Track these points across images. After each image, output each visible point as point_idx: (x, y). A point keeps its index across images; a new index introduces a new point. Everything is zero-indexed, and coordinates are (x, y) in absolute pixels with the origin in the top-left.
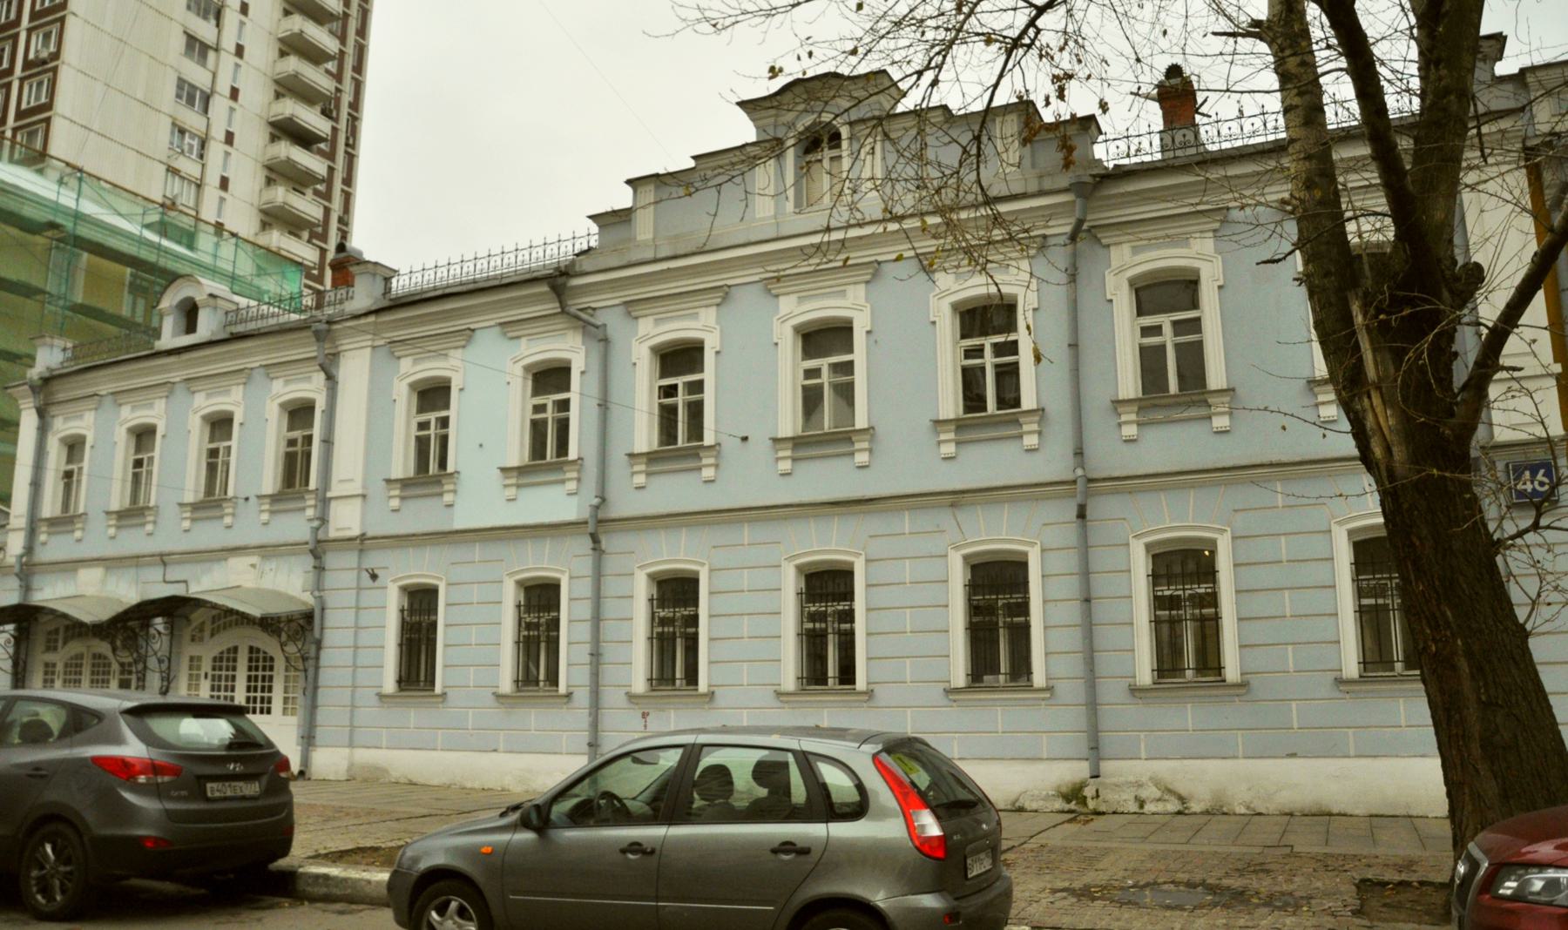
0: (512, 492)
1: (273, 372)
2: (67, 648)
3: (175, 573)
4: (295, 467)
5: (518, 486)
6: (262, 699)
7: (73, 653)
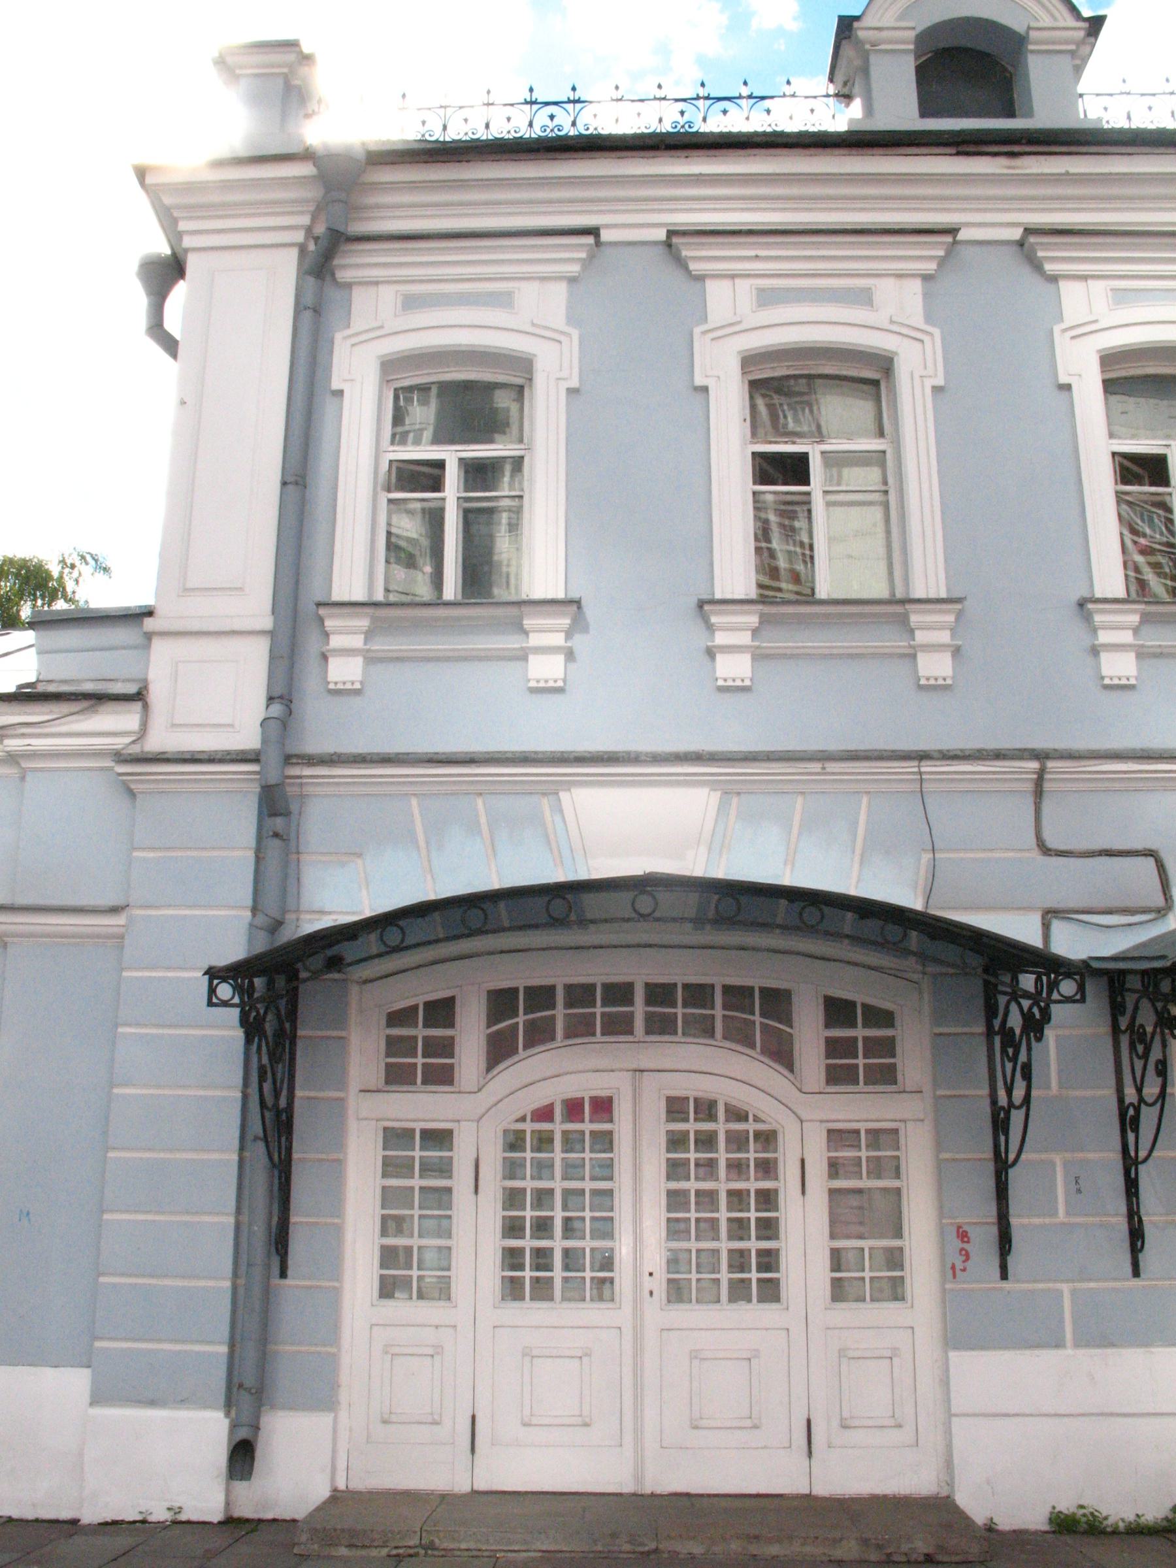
2: (512, 1073)
7: (555, 1092)
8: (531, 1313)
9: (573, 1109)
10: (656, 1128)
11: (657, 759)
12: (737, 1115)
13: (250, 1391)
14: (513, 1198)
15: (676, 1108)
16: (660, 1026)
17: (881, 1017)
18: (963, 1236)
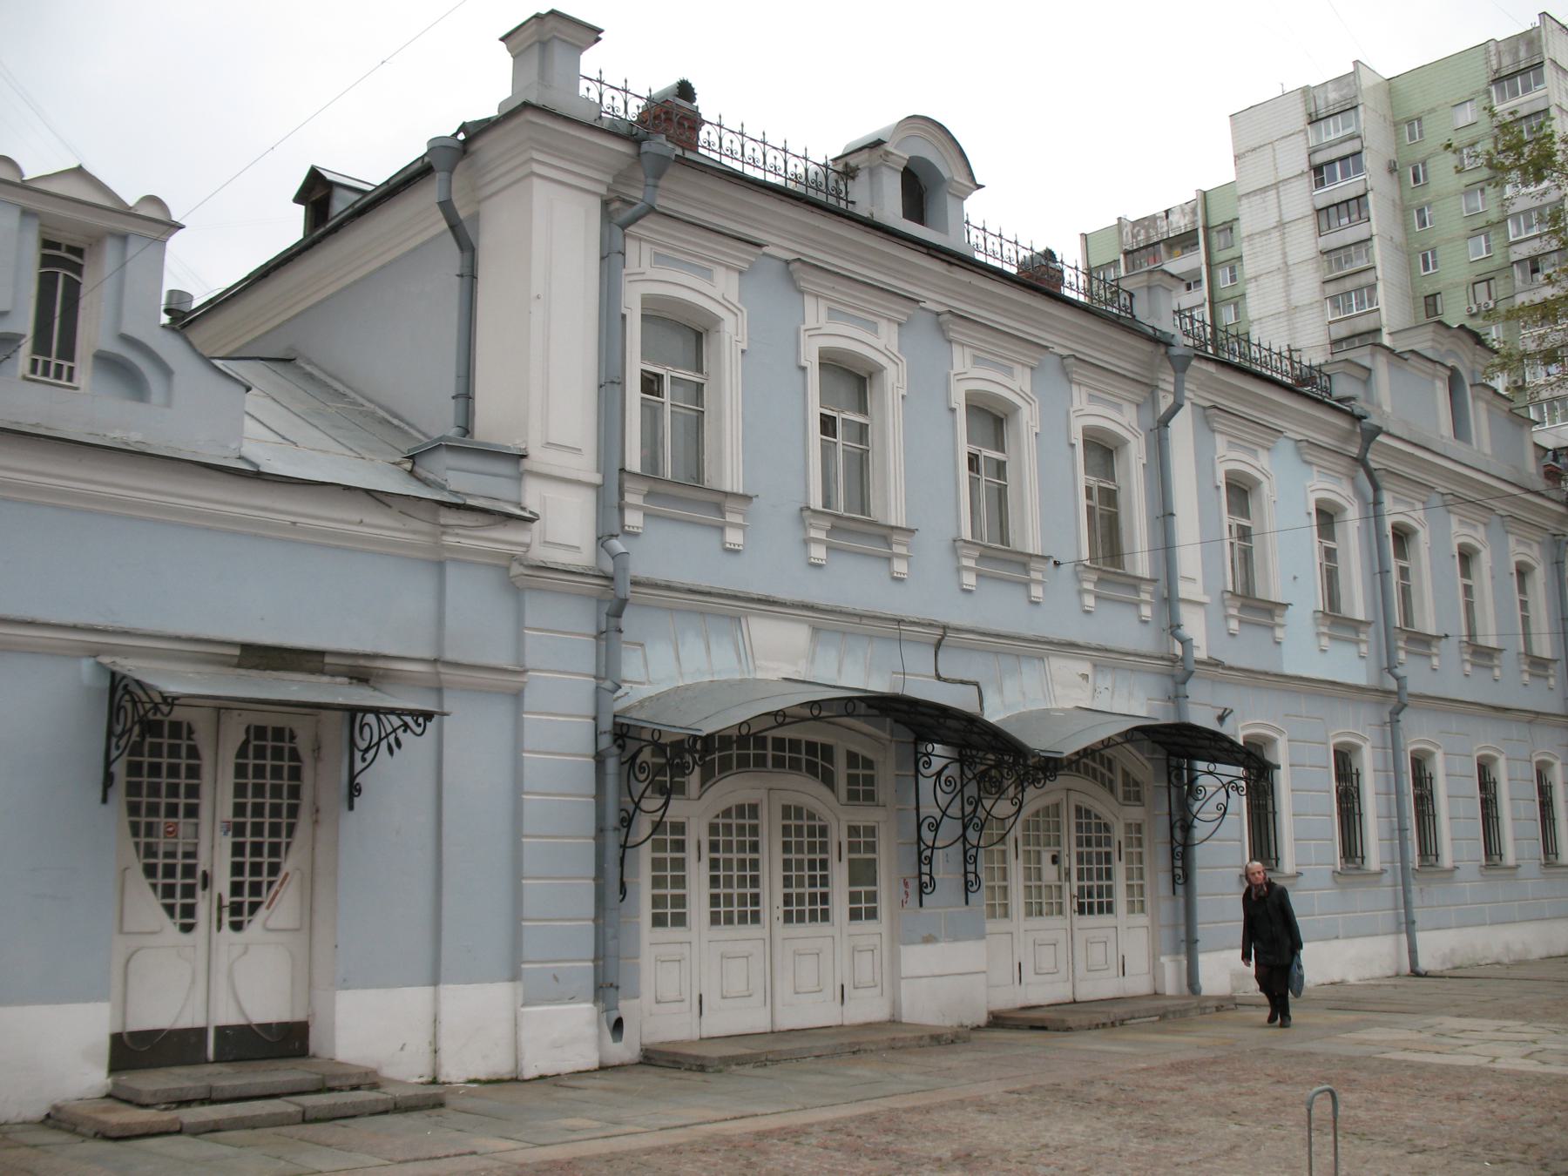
0: (1325, 641)
3: (952, 665)
5: (1332, 638)
7: (733, 800)
8: (724, 931)
9: (741, 810)
10: (779, 823)
11: (794, 605)
14: (714, 864)
16: (779, 763)
17: (869, 764)
18: (906, 884)
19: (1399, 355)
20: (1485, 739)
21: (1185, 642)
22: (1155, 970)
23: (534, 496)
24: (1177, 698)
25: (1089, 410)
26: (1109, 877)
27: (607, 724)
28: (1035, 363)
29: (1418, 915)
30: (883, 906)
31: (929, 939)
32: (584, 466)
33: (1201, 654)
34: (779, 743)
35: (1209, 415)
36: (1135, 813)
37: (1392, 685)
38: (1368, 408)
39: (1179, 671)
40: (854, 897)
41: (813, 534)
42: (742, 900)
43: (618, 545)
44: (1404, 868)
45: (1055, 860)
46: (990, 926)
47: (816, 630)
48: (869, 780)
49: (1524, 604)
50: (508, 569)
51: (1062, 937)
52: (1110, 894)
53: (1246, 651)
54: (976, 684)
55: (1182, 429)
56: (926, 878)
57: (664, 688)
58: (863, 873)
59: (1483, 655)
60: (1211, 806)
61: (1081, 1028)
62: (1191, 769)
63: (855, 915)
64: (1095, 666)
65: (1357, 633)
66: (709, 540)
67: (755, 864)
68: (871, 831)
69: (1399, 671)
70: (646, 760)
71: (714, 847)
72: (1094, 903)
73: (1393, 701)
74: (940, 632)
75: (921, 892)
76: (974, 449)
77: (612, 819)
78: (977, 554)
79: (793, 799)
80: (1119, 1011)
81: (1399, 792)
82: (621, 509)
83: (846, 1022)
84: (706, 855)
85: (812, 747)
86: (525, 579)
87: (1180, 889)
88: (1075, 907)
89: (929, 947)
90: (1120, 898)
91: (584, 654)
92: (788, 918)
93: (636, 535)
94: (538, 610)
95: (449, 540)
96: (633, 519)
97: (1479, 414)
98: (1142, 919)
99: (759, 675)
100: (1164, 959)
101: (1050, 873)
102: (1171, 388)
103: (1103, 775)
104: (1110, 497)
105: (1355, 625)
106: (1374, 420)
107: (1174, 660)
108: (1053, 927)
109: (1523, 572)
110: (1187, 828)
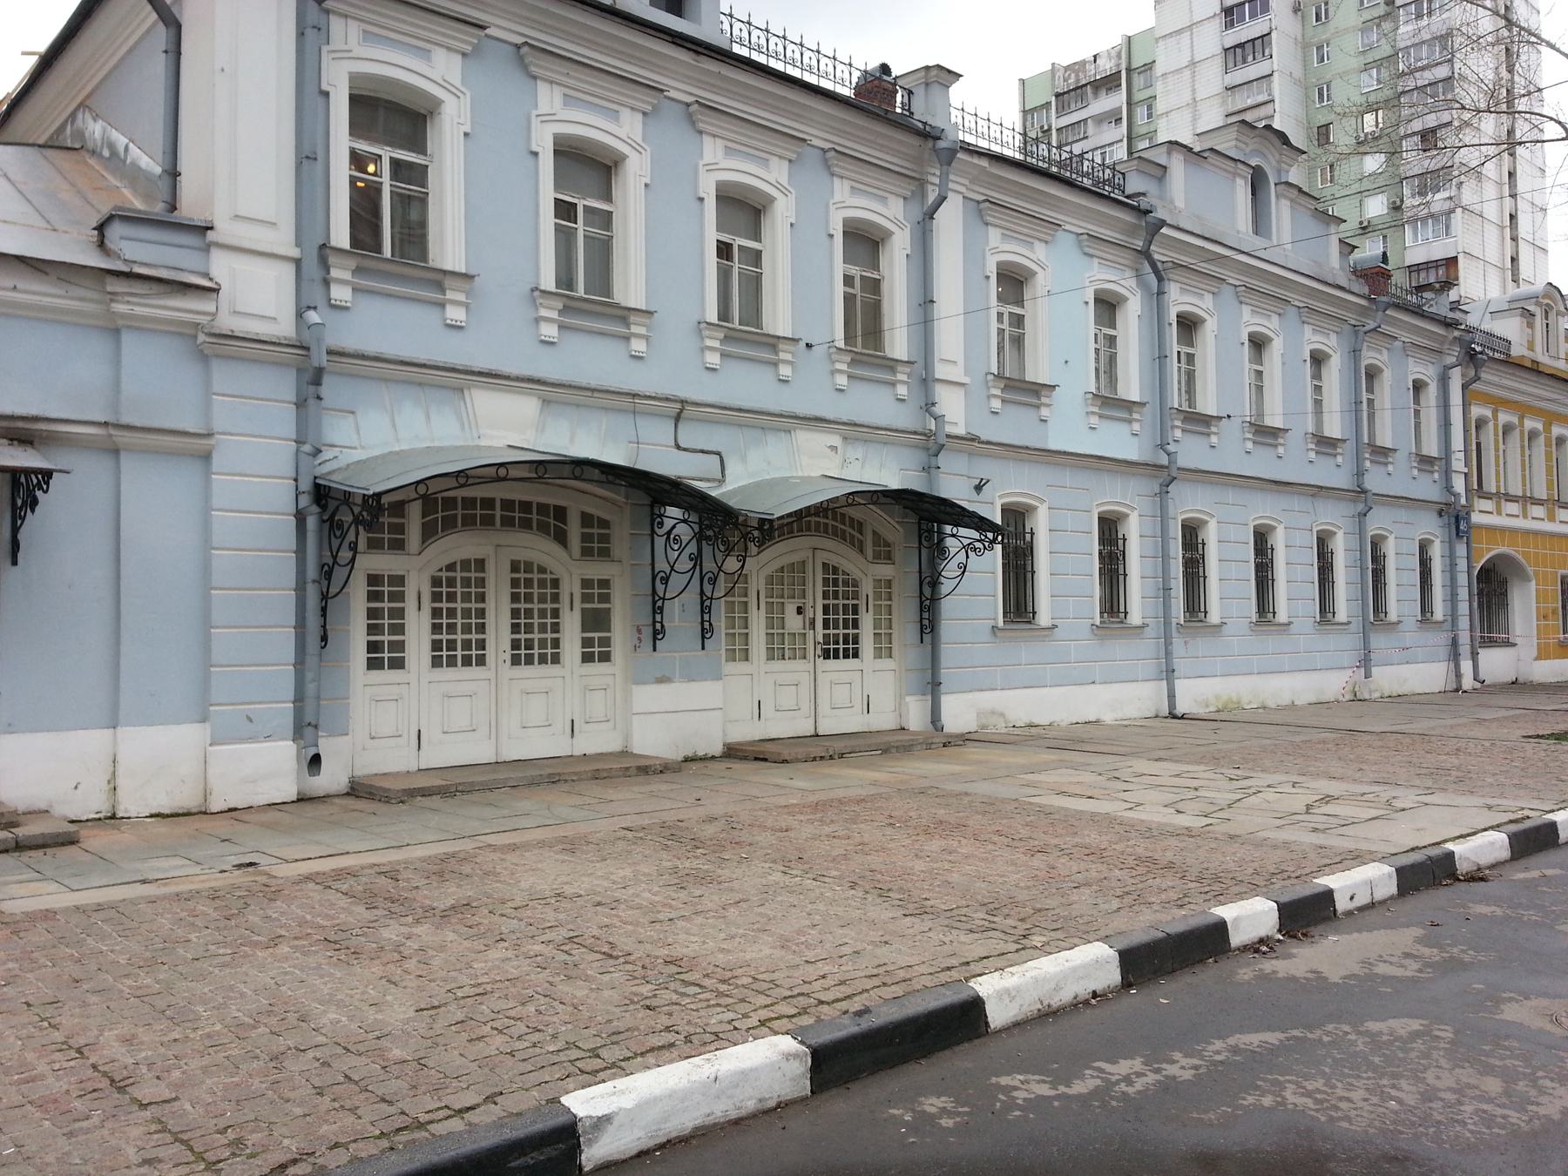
0: (1094, 420)
1: (840, 166)
3: (691, 435)
4: (865, 317)
5: (1101, 416)
6: (846, 637)
8: (447, 673)
9: (466, 564)
10: (507, 576)
11: (518, 379)
12: (542, 570)
13: (304, 727)
14: (436, 613)
15: (515, 567)
16: (508, 522)
17: (604, 524)
18: (639, 631)
19: (1197, 154)
20: (1262, 509)
21: (938, 418)
22: (900, 710)
23: (221, 267)
24: (929, 469)
25: (847, 201)
26: (856, 626)
27: (306, 485)
28: (793, 157)
29: (1178, 664)
30: (618, 648)
31: (662, 680)
32: (283, 240)
33: (960, 430)
34: (469, 503)
35: (982, 210)
36: (885, 571)
37: (1164, 460)
38: (1154, 201)
39: (932, 444)
40: (587, 642)
41: (543, 313)
42: (467, 645)
43: (313, 317)
44: (1167, 623)
45: (800, 611)
46: (730, 668)
47: (546, 402)
48: (605, 539)
49: (1318, 389)
50: (196, 337)
51: (806, 679)
52: (856, 641)
53: (1014, 426)
54: (718, 454)
55: (951, 220)
56: (658, 626)
57: (377, 452)
58: (596, 621)
59: (1266, 434)
60: (953, 565)
61: (798, 760)
62: (940, 532)
63: (587, 658)
64: (845, 438)
65: (1130, 412)
66: (429, 316)
67: (481, 613)
68: (605, 583)
69: (1171, 448)
70: (341, 520)
71: (436, 597)
72: (842, 647)
73: (1163, 475)
74: (679, 406)
75: (655, 639)
76: (726, 238)
77: (312, 572)
78: (722, 336)
79: (522, 555)
80: (839, 746)
81: (1165, 557)
82: (326, 283)
83: (576, 753)
84: (427, 605)
85: (543, 509)
86: (218, 346)
87: (927, 638)
88: (819, 652)
89: (663, 688)
90: (867, 645)
91: (284, 419)
92: (515, 661)
93: (347, 308)
94: (224, 376)
95: (120, 308)
96: (340, 293)
97: (1282, 212)
98: (886, 663)
99: (483, 443)
100: (908, 699)
101: (794, 623)
102: (937, 181)
103: (852, 536)
104: (874, 286)
105: (1129, 405)
106: (1160, 214)
107: (928, 435)
108: (797, 670)
109: (1318, 359)
110: (935, 584)
